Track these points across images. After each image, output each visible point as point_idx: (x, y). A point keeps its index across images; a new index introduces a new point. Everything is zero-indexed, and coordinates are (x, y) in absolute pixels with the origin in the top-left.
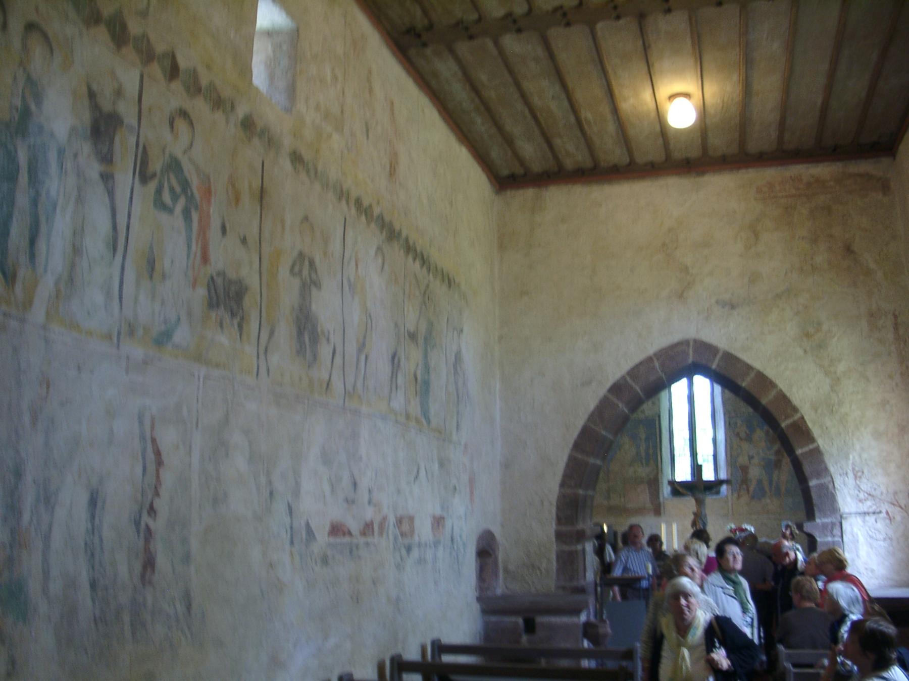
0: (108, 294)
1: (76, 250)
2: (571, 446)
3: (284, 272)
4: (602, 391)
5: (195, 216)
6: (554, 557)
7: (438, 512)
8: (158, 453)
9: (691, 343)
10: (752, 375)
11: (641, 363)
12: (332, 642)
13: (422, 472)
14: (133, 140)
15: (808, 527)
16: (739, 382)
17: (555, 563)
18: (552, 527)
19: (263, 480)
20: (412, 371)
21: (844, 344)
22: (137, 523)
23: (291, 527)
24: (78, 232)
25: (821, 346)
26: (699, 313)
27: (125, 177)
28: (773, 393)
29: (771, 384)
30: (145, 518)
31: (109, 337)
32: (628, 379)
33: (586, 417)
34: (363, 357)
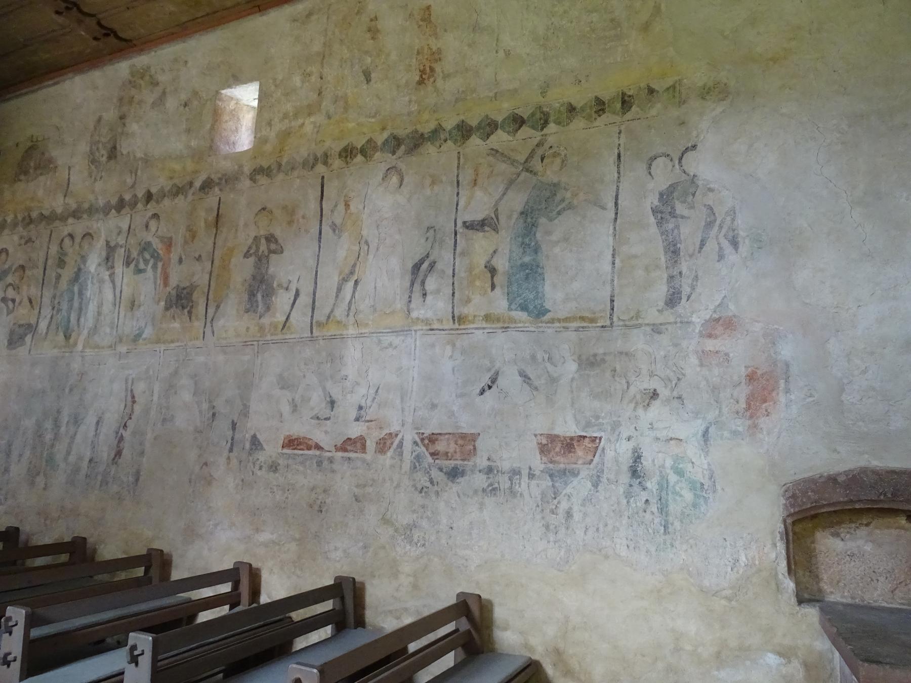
0: (112, 328)
1: (99, 314)
3: (237, 260)
5: (160, 265)
7: (569, 428)
8: (133, 397)
12: (265, 536)
13: (510, 380)
14: (123, 250)
19: (205, 406)
20: (482, 262)
22: (117, 433)
23: (233, 439)
24: (100, 306)
27: (119, 269)
30: (122, 431)
31: (111, 347)
34: (351, 284)
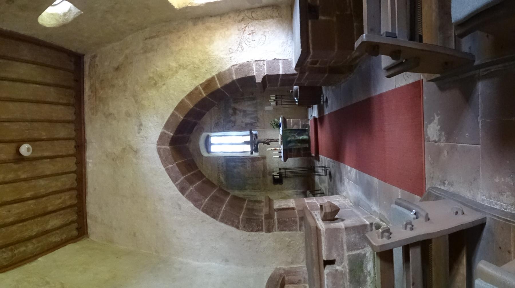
2: (214, 220)
4: (184, 198)
6: (282, 232)
9: (159, 147)
10: (177, 113)
11: (169, 175)
15: (259, 80)
16: (180, 120)
17: (286, 232)
18: (263, 234)
21: (161, 64)
25: (161, 76)
26: (144, 142)
28: (187, 101)
29: (182, 102)
32: (177, 183)
33: (198, 210)
